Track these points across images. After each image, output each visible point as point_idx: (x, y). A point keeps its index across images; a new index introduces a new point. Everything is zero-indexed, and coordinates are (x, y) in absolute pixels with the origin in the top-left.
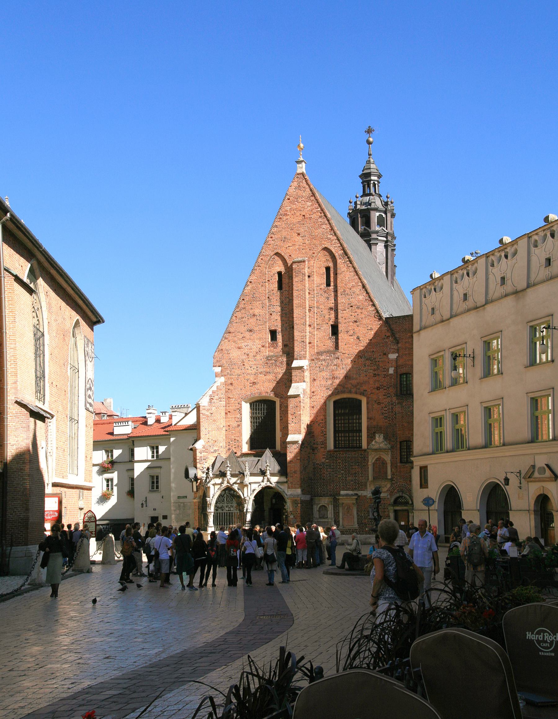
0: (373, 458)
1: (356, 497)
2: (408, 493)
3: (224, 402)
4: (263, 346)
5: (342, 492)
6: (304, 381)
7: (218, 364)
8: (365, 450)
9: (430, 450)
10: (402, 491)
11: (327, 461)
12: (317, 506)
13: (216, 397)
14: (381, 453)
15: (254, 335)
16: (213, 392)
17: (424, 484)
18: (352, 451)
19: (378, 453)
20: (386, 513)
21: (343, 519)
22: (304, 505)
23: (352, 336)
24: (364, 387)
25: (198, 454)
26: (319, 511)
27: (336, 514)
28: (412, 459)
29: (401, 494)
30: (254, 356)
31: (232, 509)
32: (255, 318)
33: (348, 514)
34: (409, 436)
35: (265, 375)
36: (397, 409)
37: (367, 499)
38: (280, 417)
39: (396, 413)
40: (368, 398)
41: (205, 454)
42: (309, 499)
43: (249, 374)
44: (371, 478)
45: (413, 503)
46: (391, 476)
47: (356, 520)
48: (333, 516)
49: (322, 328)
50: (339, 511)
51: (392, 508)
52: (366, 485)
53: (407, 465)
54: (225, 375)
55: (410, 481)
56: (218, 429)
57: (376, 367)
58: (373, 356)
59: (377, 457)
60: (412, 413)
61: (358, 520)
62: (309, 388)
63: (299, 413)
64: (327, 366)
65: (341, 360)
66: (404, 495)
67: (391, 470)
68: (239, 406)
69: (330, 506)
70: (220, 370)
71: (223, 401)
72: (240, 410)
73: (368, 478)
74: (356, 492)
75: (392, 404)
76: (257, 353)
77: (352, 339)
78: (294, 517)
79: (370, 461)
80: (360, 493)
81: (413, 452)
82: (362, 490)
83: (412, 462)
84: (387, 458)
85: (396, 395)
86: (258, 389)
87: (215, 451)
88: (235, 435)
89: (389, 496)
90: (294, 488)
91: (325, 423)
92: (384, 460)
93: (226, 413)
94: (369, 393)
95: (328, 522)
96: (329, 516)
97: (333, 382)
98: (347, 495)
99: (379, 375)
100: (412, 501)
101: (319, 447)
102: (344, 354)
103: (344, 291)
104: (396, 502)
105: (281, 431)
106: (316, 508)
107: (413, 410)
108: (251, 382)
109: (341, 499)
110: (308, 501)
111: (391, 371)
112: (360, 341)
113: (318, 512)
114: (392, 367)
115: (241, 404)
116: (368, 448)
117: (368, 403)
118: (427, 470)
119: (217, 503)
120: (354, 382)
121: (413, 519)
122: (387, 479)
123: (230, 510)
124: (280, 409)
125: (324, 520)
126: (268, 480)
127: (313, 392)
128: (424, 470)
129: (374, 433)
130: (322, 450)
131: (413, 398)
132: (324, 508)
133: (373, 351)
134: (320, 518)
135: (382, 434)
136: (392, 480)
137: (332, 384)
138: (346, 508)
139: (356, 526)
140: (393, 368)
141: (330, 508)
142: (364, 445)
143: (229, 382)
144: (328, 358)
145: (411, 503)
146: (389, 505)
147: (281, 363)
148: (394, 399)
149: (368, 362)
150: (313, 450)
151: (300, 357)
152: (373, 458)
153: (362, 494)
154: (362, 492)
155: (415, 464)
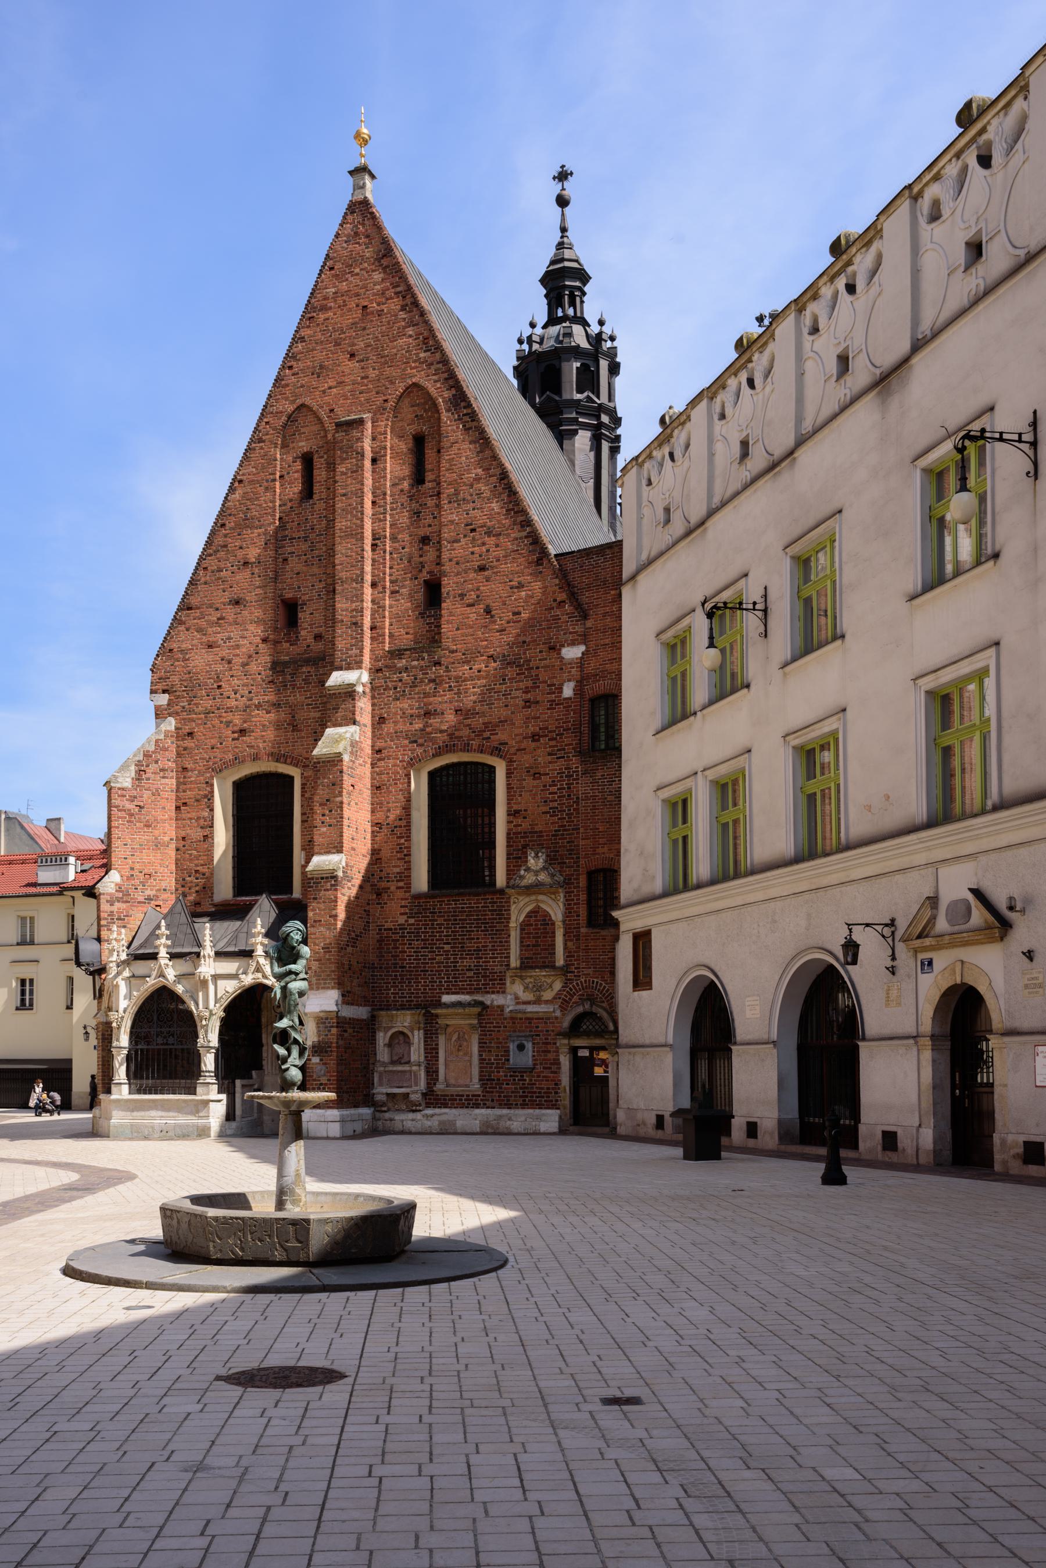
0: (520, 911)
1: (477, 1010)
2: (605, 1005)
3: (174, 781)
5: (446, 998)
6: (354, 724)
7: (160, 687)
8: (502, 892)
9: (658, 887)
10: (591, 999)
11: (412, 921)
12: (386, 1034)
13: (153, 767)
14: (541, 897)
15: (245, 613)
16: (147, 755)
17: (642, 979)
18: (469, 894)
19: (533, 897)
20: (551, 1056)
21: (446, 1065)
22: (350, 1031)
23: (473, 605)
24: (502, 736)
25: (105, 907)
26: (390, 1045)
27: (432, 1053)
28: (615, 914)
29: (587, 1006)
30: (244, 665)
31: (171, 1040)
32: (248, 571)
33: (461, 1053)
34: (612, 856)
36: (582, 787)
37: (505, 1019)
38: (303, 814)
39: (578, 798)
40: (510, 762)
41: (124, 906)
42: (365, 1017)
43: (230, 710)
44: (514, 962)
45: (616, 1031)
46: (566, 961)
47: (475, 1071)
48: (422, 1059)
49: (403, 591)
50: (437, 1045)
51: (566, 1041)
52: (502, 980)
53: (604, 933)
54: (177, 713)
55: (613, 973)
56: (158, 845)
57: (530, 683)
58: (525, 653)
59: (528, 909)
60: (619, 797)
61: (481, 1072)
62: (369, 742)
63: (338, 799)
64: (414, 686)
65: (447, 667)
66: (595, 1009)
67: (565, 945)
69: (416, 1033)
70: (165, 702)
71: (172, 778)
72: (210, 797)
74: (479, 998)
75: (569, 776)
76: (250, 657)
77: (473, 615)
78: (321, 1060)
79: (513, 918)
81: (618, 898)
82: (493, 993)
83: (616, 924)
84: (556, 910)
85: (580, 753)
86: (252, 747)
87: (149, 899)
88: (196, 862)
89: (558, 1013)
90: (323, 988)
91: (408, 825)
92: (546, 915)
93: (178, 808)
94: (513, 750)
95: (410, 1071)
96: (414, 1058)
97: (426, 725)
99: (538, 702)
100: (616, 1023)
101: (393, 888)
102: (453, 652)
104: (575, 1028)
105: (303, 849)
106: (382, 1038)
107: (619, 790)
108: (236, 729)
109: (445, 1016)
110: (363, 1020)
111: (568, 691)
112: (492, 617)
113: (386, 1049)
114: (569, 680)
115: (212, 785)
116: (508, 887)
117: (509, 774)
118: (650, 941)
120: (478, 722)
121: (618, 1069)
122: (553, 967)
123: (167, 1044)
124: (302, 796)
125: (400, 1068)
126: (258, 969)
127: (379, 751)
128: (642, 940)
129: (525, 847)
130: (400, 894)
131: (620, 757)
132: (401, 1038)
133: (524, 642)
134: (393, 1062)
135: (544, 850)
136: (565, 970)
137: (422, 730)
138: (454, 1038)
139: (476, 1086)
140: (572, 684)
141: (416, 1037)
142: (501, 879)
143: (187, 729)
144: (416, 663)
145: (611, 1027)
146: (559, 1034)
147: (306, 681)
148: (575, 763)
149: (511, 672)
150: (379, 894)
151: (349, 664)
152: (520, 911)
153: (492, 1001)
154: (493, 996)
155: (622, 928)
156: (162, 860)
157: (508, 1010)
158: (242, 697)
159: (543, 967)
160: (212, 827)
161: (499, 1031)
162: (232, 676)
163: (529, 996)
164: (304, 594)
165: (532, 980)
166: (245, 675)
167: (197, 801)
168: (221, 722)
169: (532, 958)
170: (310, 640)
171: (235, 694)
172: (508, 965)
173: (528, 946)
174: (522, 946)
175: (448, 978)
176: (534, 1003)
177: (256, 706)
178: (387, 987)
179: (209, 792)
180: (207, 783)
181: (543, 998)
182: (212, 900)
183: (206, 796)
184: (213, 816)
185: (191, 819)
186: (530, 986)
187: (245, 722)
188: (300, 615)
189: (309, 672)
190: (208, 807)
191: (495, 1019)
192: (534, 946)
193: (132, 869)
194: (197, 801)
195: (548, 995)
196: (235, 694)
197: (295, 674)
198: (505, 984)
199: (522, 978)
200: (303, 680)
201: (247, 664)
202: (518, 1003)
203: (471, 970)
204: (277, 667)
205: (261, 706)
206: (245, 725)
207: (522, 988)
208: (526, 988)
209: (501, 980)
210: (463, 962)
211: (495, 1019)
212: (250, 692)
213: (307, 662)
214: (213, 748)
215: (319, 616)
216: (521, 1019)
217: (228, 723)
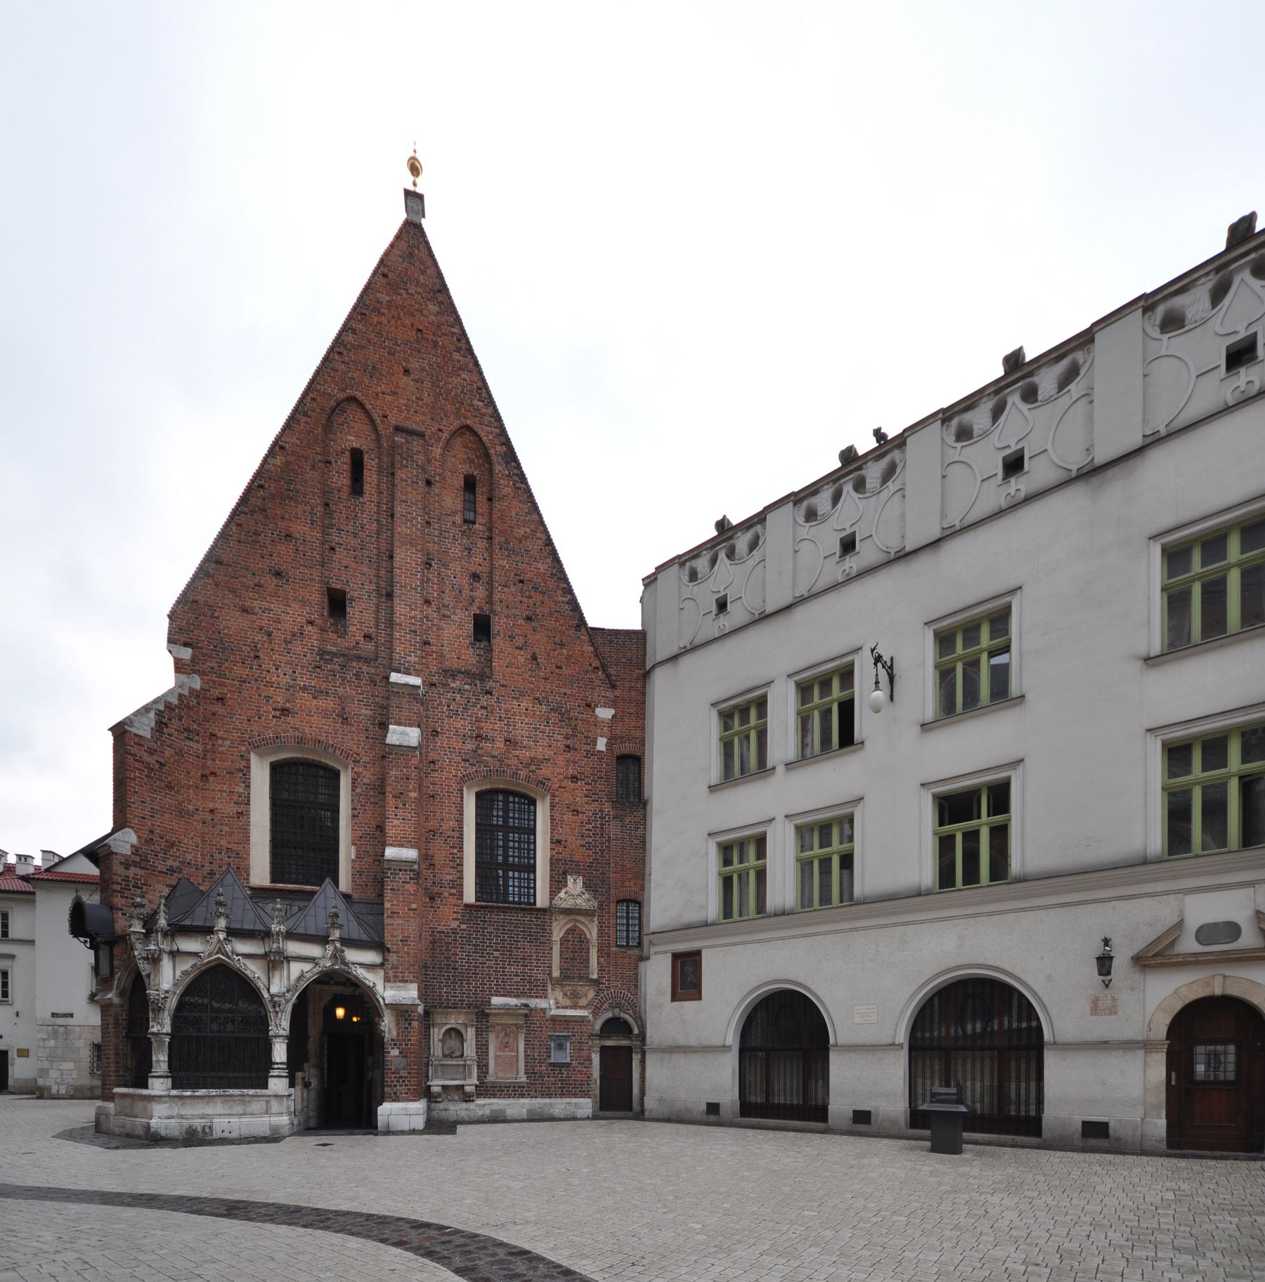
3: (200, 747)
4: (310, 623)
35: (315, 698)
37: (547, 1020)
68: (244, 763)
73: (551, 971)
74: (524, 1001)
76: (294, 636)
80: (533, 1003)
82: (537, 997)
93: (204, 777)
98: (506, 1008)
103: (507, 542)
115: (248, 760)
119: (181, 1006)
122: (585, 978)
147: (357, 675)
152: (563, 926)
154: (537, 1000)
156: (187, 830)
157: (552, 1013)
158: (285, 674)
159: (581, 978)
160: (248, 804)
161: (541, 1031)
162: (272, 650)
163: (567, 1002)
164: (354, 590)
165: (570, 988)
166: (289, 653)
167: (232, 773)
168: (260, 695)
169: (569, 970)
170: (359, 637)
171: (277, 669)
172: (550, 974)
173: (567, 958)
174: (561, 958)
175: (497, 982)
176: (571, 1008)
177: (300, 688)
178: (440, 986)
179: (245, 767)
180: (242, 756)
181: (579, 1005)
182: (248, 883)
183: (241, 770)
184: (249, 794)
185: (222, 791)
186: (568, 993)
187: (289, 702)
188: (348, 609)
189: (360, 668)
190: (244, 782)
191: (538, 1020)
192: (571, 959)
193: (152, 832)
194: (228, 773)
195: (583, 1002)
196: (277, 669)
197: (345, 666)
198: (547, 990)
199: (561, 984)
200: (354, 675)
201: (291, 643)
202: (557, 1008)
203: (518, 976)
204: (322, 653)
205: (307, 690)
206: (288, 705)
207: (561, 994)
208: (565, 995)
209: (543, 986)
210: (510, 968)
211: (538, 1020)
212: (294, 672)
213: (359, 658)
214: (249, 721)
215: (369, 617)
216: (560, 1021)
217: (268, 698)
